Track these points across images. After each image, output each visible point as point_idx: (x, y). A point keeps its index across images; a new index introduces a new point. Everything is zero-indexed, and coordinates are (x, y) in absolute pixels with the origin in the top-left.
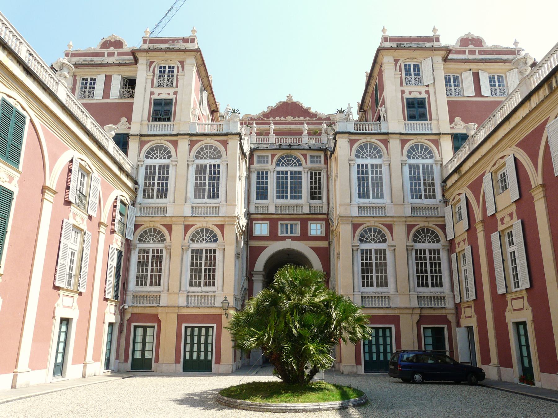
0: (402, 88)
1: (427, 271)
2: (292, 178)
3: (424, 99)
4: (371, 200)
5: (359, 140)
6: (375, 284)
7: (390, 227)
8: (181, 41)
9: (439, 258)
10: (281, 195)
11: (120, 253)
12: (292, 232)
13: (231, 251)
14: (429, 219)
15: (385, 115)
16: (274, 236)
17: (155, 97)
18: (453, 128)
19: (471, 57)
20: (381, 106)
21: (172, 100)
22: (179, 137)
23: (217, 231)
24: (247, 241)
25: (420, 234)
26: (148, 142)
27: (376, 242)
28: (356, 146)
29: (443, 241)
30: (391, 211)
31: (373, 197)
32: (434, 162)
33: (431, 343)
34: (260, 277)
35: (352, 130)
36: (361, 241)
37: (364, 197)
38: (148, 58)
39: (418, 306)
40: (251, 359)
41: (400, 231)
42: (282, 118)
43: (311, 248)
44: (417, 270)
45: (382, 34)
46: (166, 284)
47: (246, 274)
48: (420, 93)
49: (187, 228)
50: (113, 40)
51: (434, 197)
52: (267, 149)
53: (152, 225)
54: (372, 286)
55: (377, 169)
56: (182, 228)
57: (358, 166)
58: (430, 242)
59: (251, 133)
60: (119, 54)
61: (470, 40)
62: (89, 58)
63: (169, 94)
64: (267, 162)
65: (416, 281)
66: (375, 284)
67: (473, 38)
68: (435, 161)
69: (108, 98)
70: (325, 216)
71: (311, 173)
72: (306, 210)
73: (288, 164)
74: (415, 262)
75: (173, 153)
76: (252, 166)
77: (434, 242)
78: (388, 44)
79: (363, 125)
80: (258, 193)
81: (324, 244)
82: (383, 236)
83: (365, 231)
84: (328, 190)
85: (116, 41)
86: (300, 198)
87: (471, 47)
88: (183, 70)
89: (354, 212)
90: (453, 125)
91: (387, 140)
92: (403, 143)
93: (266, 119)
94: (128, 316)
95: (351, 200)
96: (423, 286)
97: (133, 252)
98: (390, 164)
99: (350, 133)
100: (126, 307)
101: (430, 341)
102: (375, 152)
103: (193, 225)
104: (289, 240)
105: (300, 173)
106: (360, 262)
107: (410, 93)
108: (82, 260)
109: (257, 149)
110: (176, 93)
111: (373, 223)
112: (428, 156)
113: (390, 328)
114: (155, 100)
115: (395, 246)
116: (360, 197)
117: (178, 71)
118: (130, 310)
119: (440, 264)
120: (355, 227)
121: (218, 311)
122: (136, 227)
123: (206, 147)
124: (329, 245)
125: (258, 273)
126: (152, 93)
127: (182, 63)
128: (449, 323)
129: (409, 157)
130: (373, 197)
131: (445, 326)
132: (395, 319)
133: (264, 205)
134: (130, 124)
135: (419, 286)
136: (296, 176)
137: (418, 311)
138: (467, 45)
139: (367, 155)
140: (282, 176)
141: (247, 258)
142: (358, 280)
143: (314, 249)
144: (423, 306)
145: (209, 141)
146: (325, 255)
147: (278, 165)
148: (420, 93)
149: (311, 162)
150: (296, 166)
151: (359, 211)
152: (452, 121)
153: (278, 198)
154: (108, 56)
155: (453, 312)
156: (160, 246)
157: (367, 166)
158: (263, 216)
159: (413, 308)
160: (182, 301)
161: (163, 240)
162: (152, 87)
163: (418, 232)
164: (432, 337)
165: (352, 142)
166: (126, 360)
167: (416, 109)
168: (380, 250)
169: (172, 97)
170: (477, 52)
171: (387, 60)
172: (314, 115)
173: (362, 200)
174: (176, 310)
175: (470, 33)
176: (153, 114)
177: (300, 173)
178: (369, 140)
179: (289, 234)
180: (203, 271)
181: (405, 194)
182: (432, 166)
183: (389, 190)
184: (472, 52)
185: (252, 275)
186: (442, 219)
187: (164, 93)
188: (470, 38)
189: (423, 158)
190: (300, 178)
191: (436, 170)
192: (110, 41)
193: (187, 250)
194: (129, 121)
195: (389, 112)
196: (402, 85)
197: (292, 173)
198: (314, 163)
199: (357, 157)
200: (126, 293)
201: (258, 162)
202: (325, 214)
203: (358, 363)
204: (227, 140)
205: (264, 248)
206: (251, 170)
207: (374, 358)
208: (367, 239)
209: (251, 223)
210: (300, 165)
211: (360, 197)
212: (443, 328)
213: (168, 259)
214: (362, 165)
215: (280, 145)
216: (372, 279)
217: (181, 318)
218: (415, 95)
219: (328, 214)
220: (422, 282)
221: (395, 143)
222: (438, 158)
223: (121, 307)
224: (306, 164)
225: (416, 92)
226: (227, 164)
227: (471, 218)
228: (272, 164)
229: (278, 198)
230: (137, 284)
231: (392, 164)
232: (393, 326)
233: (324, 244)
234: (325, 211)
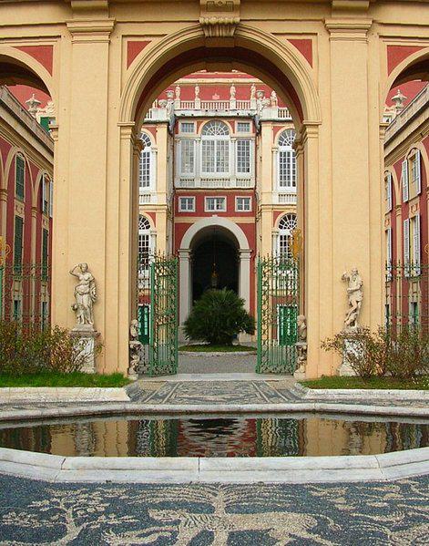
16: (200, 213)
23: (149, 218)
34: (187, 255)
35: (276, 118)
36: (281, 227)
52: (193, 118)
71: (239, 143)
72: (233, 185)
76: (176, 135)
81: (251, 220)
83: (285, 218)
89: (275, 200)
99: (274, 121)
104: (215, 216)
109: (183, 117)
120: (276, 214)
125: (184, 250)
146: (251, 231)
149: (239, 130)
165: (275, 130)
177: (227, 142)
179: (215, 210)
197: (218, 143)
209: (177, 199)
210: (227, 133)
233: (251, 220)
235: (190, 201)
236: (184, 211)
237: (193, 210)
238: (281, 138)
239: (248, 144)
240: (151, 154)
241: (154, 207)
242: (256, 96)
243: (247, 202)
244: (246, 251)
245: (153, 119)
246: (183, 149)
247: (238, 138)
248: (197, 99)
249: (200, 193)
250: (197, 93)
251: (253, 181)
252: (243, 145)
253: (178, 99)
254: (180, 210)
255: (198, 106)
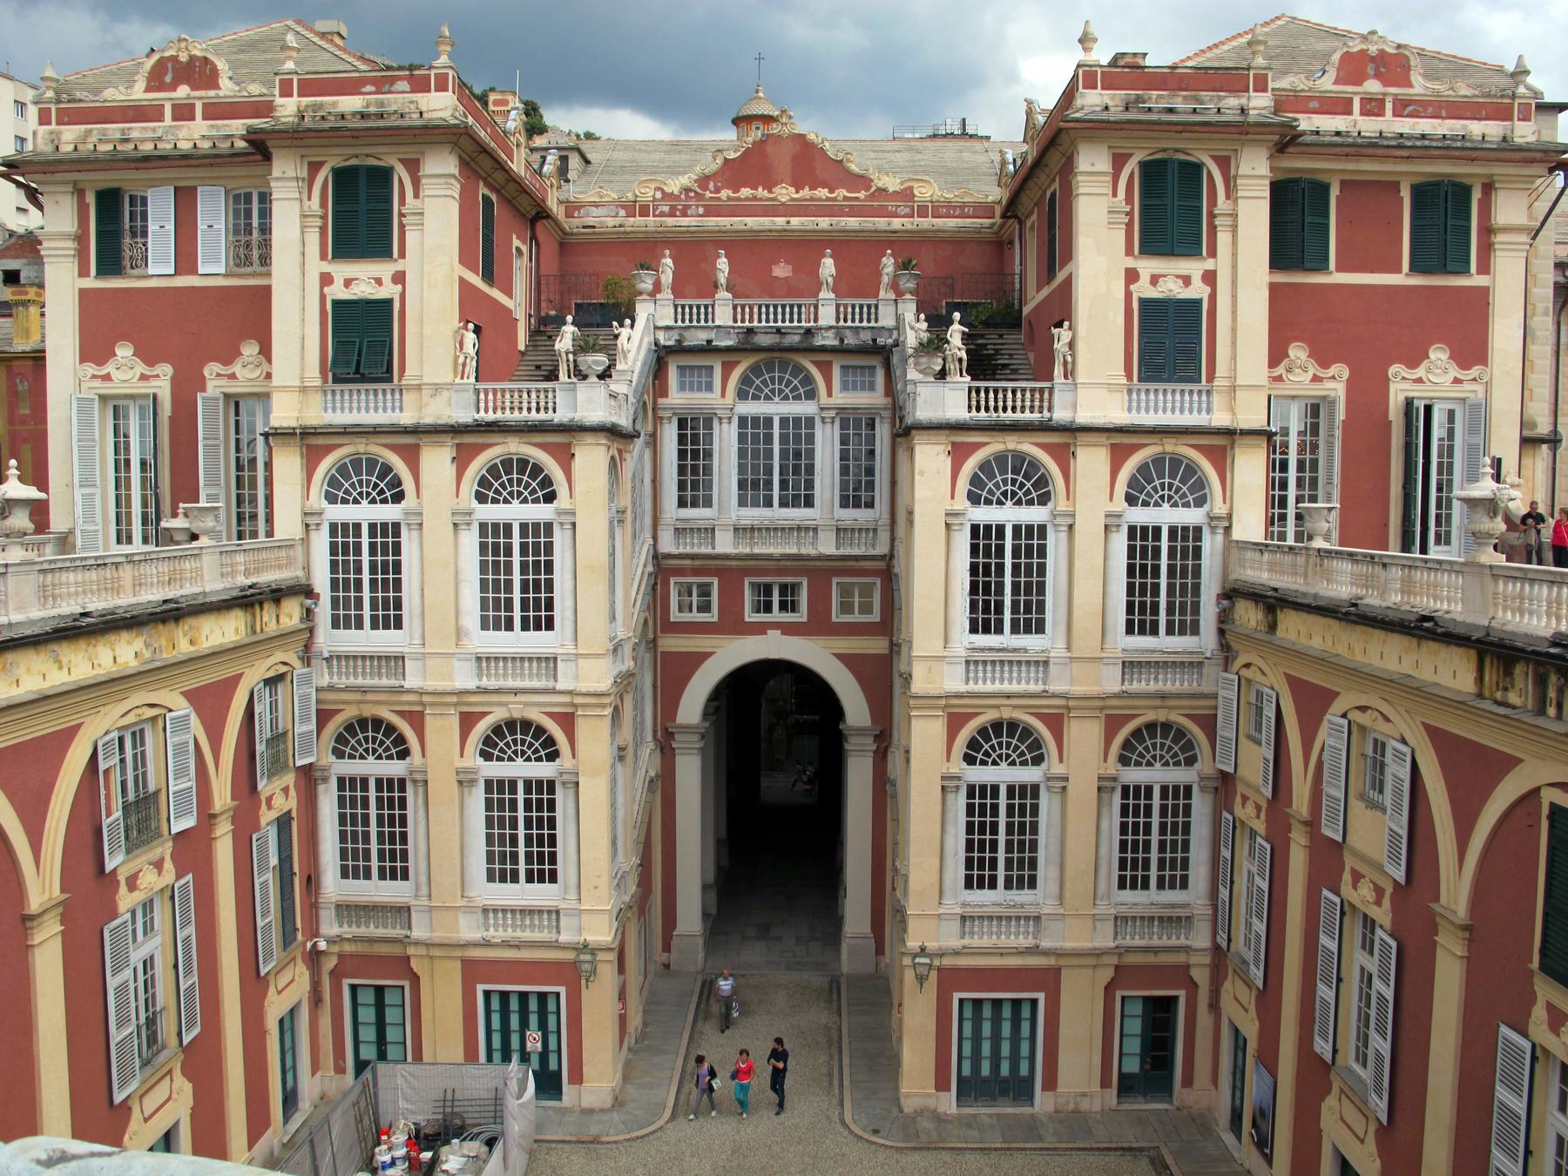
0: (1130, 263)
1: (1147, 842)
2: (784, 439)
3: (1197, 303)
4: (1006, 639)
5: (978, 446)
6: (1001, 881)
7: (1055, 723)
8: (403, 85)
9: (1187, 810)
10: (752, 488)
11: (284, 822)
12: (783, 606)
13: (595, 791)
14: (1170, 703)
15: (1069, 359)
16: (732, 625)
17: (337, 292)
18: (1279, 379)
19: (1369, 126)
20: (1059, 325)
21: (387, 303)
22: (426, 439)
24: (655, 640)
25: (1145, 738)
26: (330, 449)
27: (1013, 763)
28: (970, 465)
29: (1204, 766)
30: (1059, 683)
31: (1015, 629)
32: (1206, 520)
33: (1139, 1031)
34: (694, 741)
36: (970, 760)
37: (986, 631)
38: (302, 151)
39: (1112, 945)
40: (674, 956)
41: (1085, 736)
42: (761, 192)
43: (839, 656)
44: (1123, 844)
45: (1080, 55)
46: (423, 879)
47: (655, 732)
48: (1187, 280)
49: (468, 721)
50: (184, 58)
51: (1195, 631)
52: (708, 349)
53: (368, 711)
54: (993, 886)
55: (1032, 536)
56: (455, 722)
57: (975, 529)
58: (1167, 764)
59: (657, 287)
60: (215, 111)
61: (1372, 59)
62: (114, 129)
63: (379, 281)
64: (709, 388)
65: (1116, 873)
66: (1001, 881)
67: (1382, 52)
68: (1212, 519)
69: (193, 270)
70: (881, 565)
71: (844, 425)
72: (827, 546)
73: (773, 391)
74: (1117, 819)
75: (408, 485)
76: (661, 401)
77: (1177, 764)
78: (1092, 100)
79: (996, 392)
80: (682, 486)
82: (1037, 745)
83: (983, 731)
84: (893, 483)
85: (192, 58)
86: (809, 503)
87: (1373, 86)
88: (416, 196)
89: (953, 681)
90: (1280, 370)
91: (1068, 445)
92: (1118, 456)
93: (708, 194)
94: (330, 963)
95: (946, 641)
96: (1134, 887)
97: (321, 788)
98: (1071, 527)
100: (322, 945)
101: (1134, 1046)
102: (1029, 485)
103: (485, 714)
104: (774, 634)
105: (810, 421)
106: (962, 818)
107: (1154, 280)
108: (176, 966)
109: (680, 349)
110: (399, 278)
111: (1007, 714)
112: (1190, 498)
113: (1034, 1002)
114: (336, 303)
115: (1067, 779)
116: (974, 630)
117: (402, 201)
118: (335, 949)
119: (1187, 828)
120: (955, 722)
121: (570, 956)
122: (323, 717)
123: (507, 463)
124: (894, 648)
125: (687, 729)
126: (326, 279)
127: (413, 166)
128: (1192, 986)
129: (1131, 500)
130: (1015, 629)
131: (1182, 994)
132: (1049, 979)
133: (702, 525)
134: (269, 361)
135: (1122, 886)
136: (799, 432)
137: (1114, 960)
138: (1358, 83)
139: (1005, 494)
140: (753, 431)
141: (655, 687)
142: (956, 870)
143: (847, 659)
144: (1128, 942)
145: (515, 447)
147: (742, 395)
148: (1187, 280)
150: (797, 398)
151: (968, 671)
152: (1277, 355)
153: (742, 502)
154: (175, 119)
155: (1207, 960)
156: (394, 768)
157: (1001, 529)
158: (697, 563)
159: (1099, 954)
160: (468, 929)
161: (404, 754)
162: (323, 257)
163: (1137, 734)
164: (1143, 1016)
165: (959, 454)
166: (340, 1070)
167: (1170, 341)
168: (1023, 787)
169: (389, 291)
170: (1389, 106)
171: (1092, 162)
172: (862, 181)
173: (982, 640)
174: (458, 953)
175: (1373, 33)
176: (335, 352)
178: (1011, 446)
180: (526, 837)
181: (1110, 622)
182: (1198, 530)
183: (1063, 611)
184: (1373, 107)
185: (669, 735)
186: (1211, 703)
187: (364, 279)
188: (1373, 49)
189: (1175, 505)
190: (811, 439)
191: (1211, 545)
192: (174, 59)
193: (472, 782)
194: (266, 352)
195: (1081, 347)
196: (1129, 251)
197: (784, 421)
198: (855, 388)
199: (974, 499)
200: (316, 901)
201: (682, 388)
202: (882, 557)
203: (942, 1084)
204: (569, 445)
205: (705, 656)
206: (660, 413)
207: (986, 1069)
208: (987, 754)
209: (666, 584)
210: (811, 395)
211: (974, 630)
212: (1175, 998)
213: (421, 812)
214: (988, 528)
215: (750, 331)
216: (994, 831)
217: (472, 971)
218: (1171, 289)
219: (892, 556)
220: (1131, 875)
221: (1091, 461)
222: (1220, 509)
223: (309, 945)
224: (830, 394)
225: (1172, 278)
226: (574, 524)
227: (1282, 781)
228: (723, 395)
229: (742, 502)
230: (345, 875)
231: (1077, 527)
232: (1041, 997)
233: (875, 645)
234: (882, 549)
235: (705, 591)
236: (686, 617)
237: (713, 616)
238: (975, 481)
239: (871, 425)
240: (556, 529)
241: (566, 699)
242: (894, 286)
243: (866, 591)
244: (861, 731)
245: (562, 416)
246: (682, 439)
247: (841, 410)
248: (723, 295)
249: (729, 570)
250: (722, 278)
251: (884, 536)
252: (855, 425)
253: (666, 295)
254: (675, 616)
255: (723, 316)
